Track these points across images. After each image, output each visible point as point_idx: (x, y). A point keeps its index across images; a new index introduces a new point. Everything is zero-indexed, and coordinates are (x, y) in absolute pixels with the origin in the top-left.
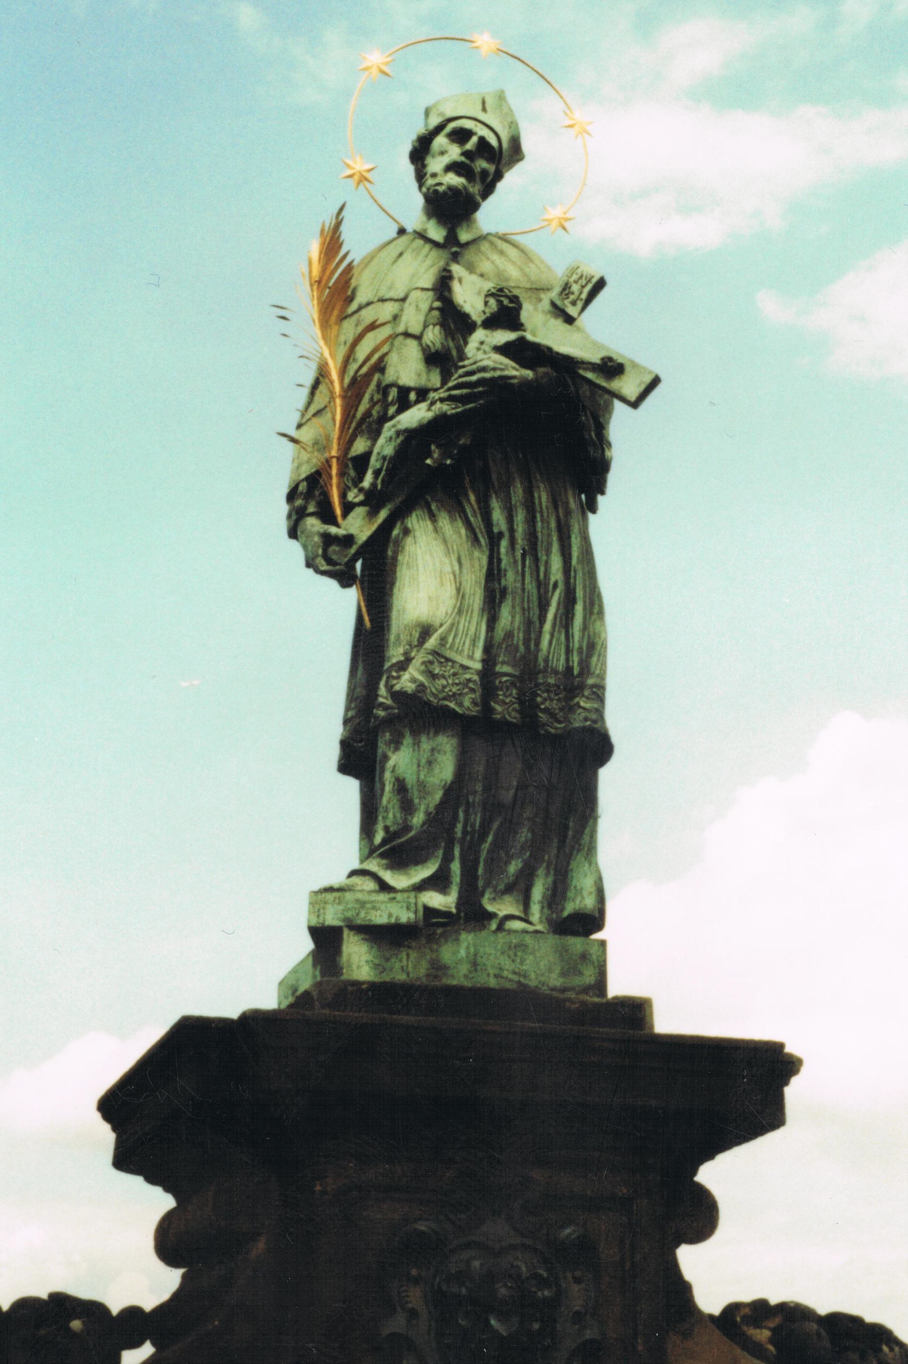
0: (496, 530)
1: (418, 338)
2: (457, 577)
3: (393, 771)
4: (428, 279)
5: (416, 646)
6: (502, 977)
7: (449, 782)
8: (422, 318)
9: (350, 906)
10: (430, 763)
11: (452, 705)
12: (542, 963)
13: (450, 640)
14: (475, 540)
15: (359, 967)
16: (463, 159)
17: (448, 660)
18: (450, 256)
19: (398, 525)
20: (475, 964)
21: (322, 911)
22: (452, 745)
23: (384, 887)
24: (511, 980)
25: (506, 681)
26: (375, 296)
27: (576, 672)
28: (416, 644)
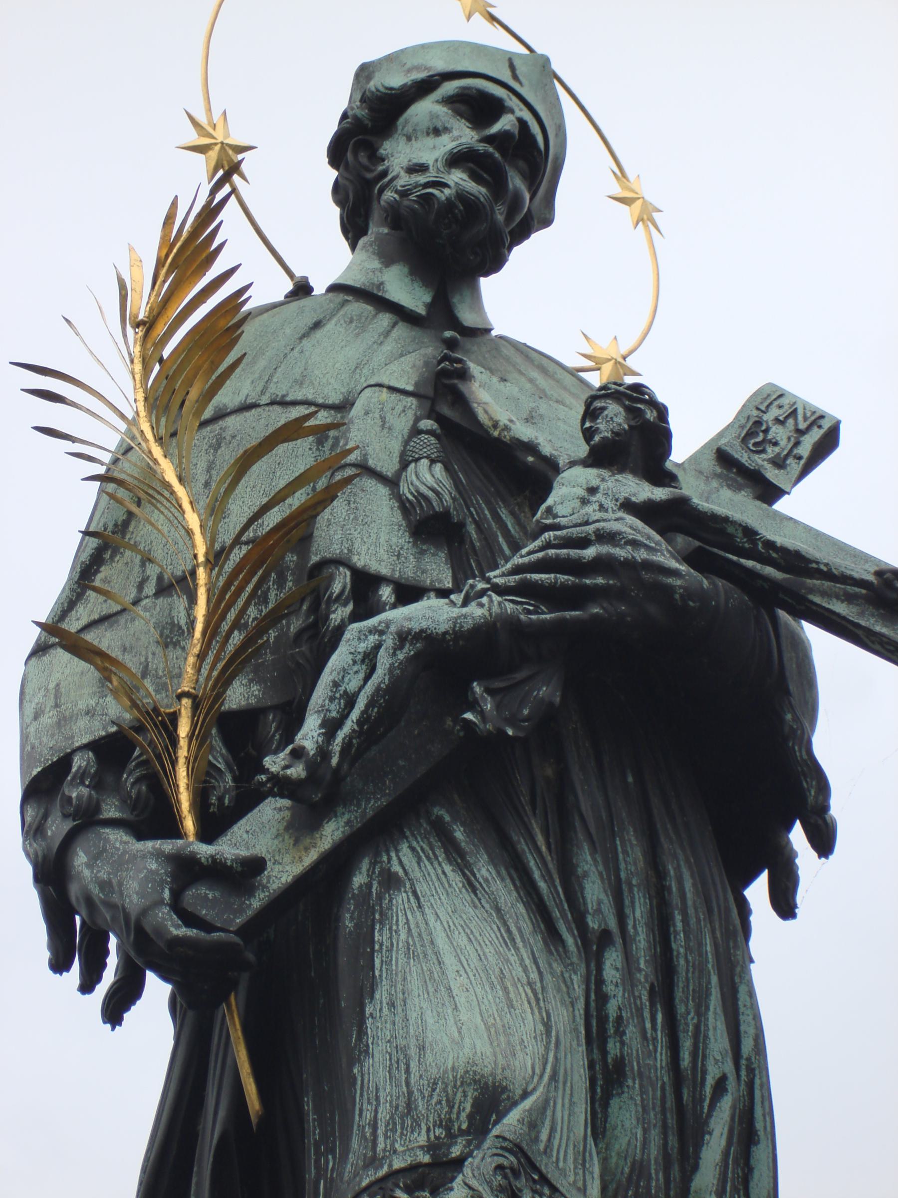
0: (593, 923)
1: (392, 483)
2: (540, 996)
5: (467, 1132)
8: (396, 446)
13: (544, 1136)
14: (552, 935)
19: (365, 864)
26: (263, 393)
28: (464, 1126)
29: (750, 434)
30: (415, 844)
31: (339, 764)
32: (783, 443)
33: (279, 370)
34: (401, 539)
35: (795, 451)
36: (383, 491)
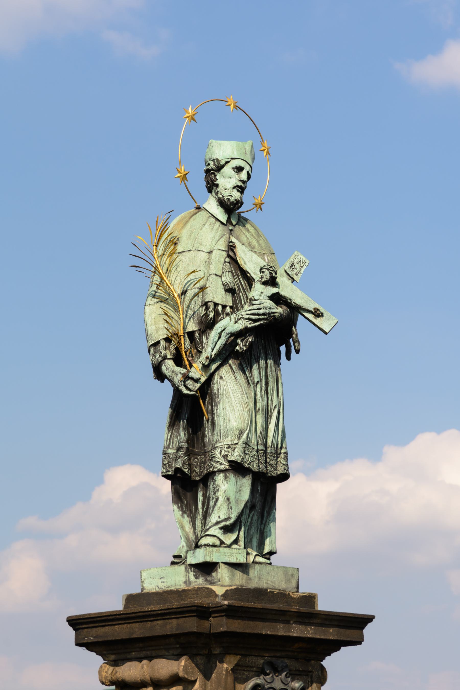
1: (221, 277)
3: (224, 493)
4: (222, 245)
6: (268, 584)
7: (247, 500)
8: (221, 266)
9: (222, 554)
10: (240, 491)
11: (251, 467)
12: (280, 578)
15: (225, 579)
16: (240, 184)
17: (249, 446)
18: (229, 231)
20: (260, 578)
21: (211, 555)
22: (249, 483)
23: (222, 542)
24: (270, 585)
25: (262, 453)
26: (193, 246)
27: (279, 447)
29: (292, 266)
30: (225, 369)
31: (214, 357)
32: (298, 269)
33: (196, 240)
34: (223, 292)
35: (300, 272)
36: (219, 279)
